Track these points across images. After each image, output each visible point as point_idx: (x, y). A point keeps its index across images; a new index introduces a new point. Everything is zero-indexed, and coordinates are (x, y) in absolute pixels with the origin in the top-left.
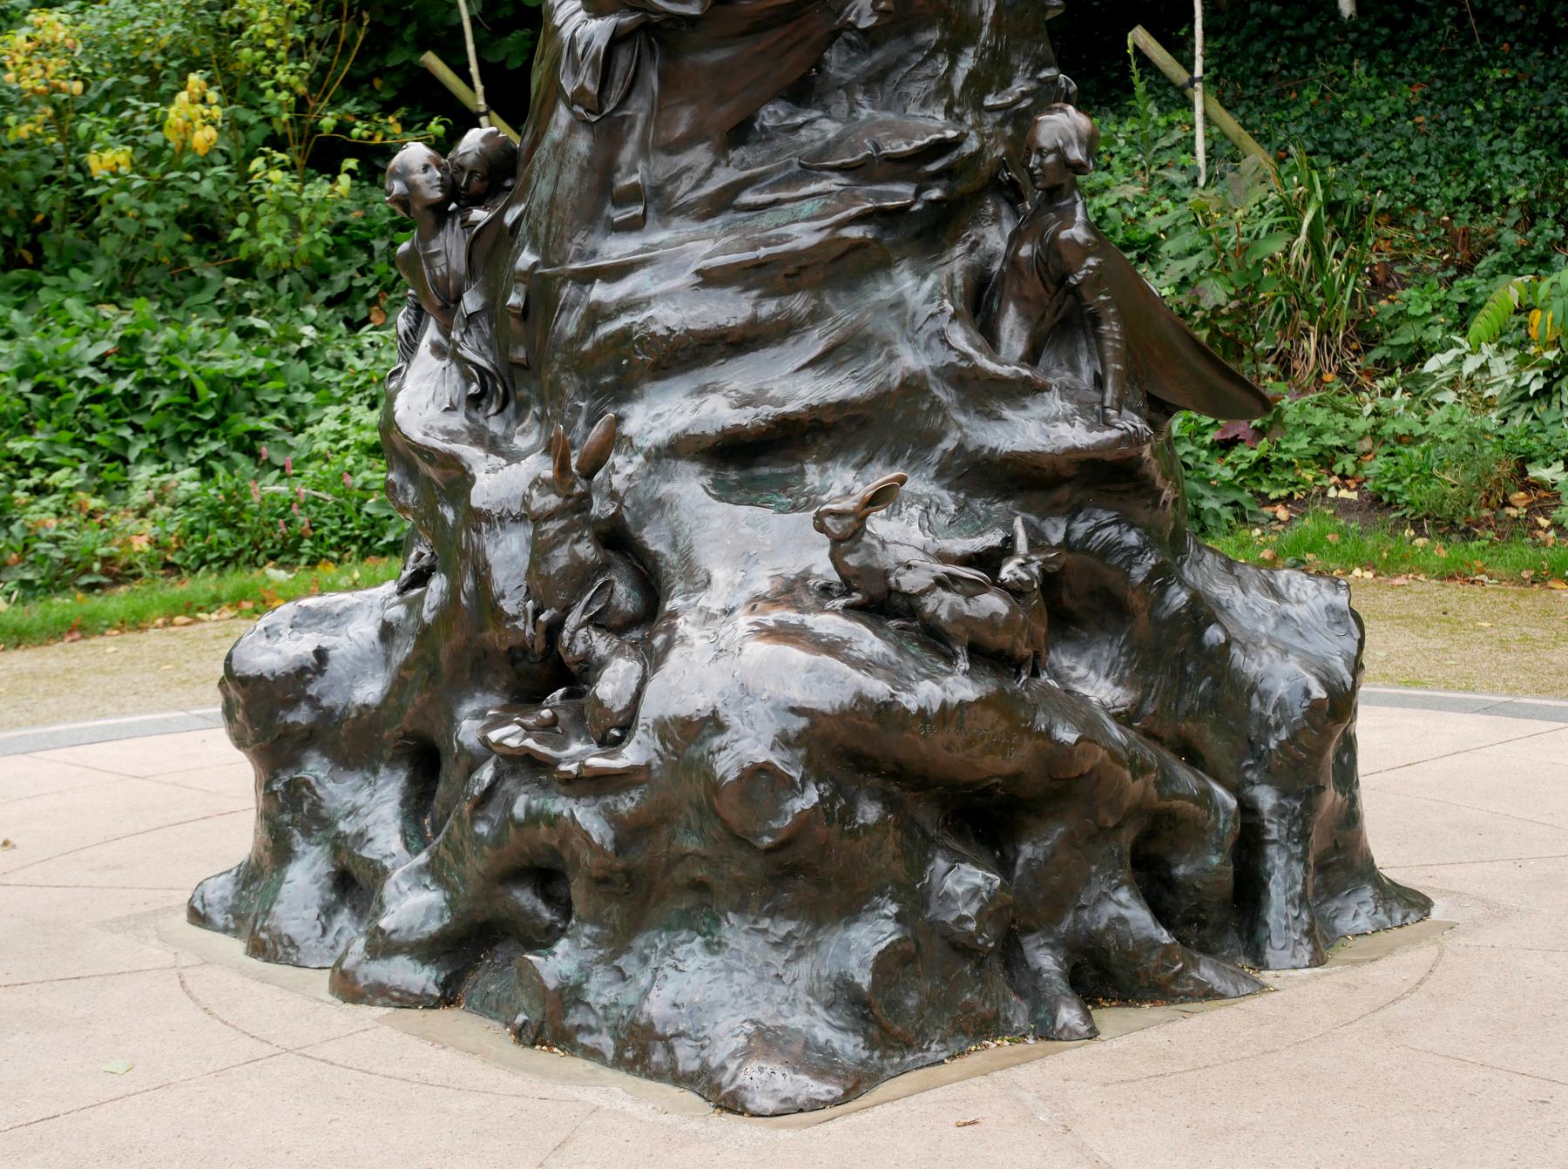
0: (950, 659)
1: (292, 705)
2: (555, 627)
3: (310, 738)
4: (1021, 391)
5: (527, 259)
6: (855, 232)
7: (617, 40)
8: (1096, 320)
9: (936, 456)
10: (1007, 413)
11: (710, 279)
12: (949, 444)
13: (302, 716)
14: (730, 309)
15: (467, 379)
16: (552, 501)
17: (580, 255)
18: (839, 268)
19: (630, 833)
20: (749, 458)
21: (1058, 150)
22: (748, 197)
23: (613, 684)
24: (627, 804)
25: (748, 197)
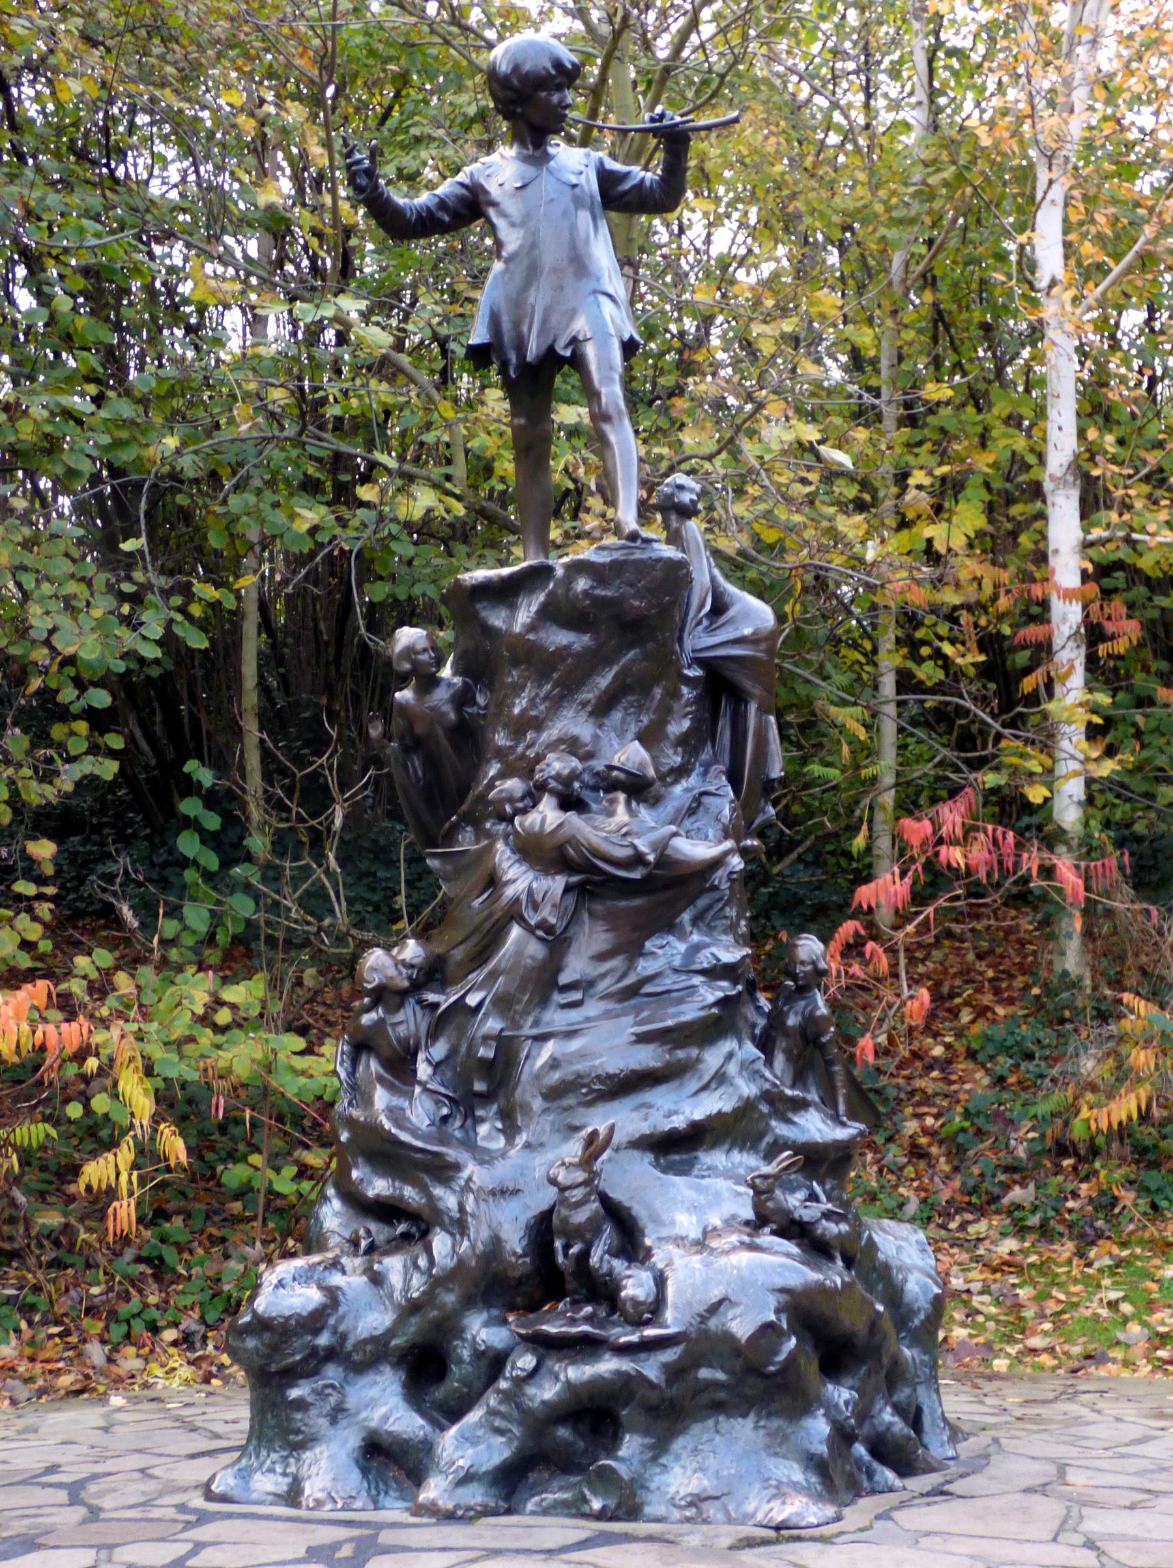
0: (831, 1259)
1: (317, 1332)
2: (585, 1254)
3: (331, 1354)
4: (800, 1105)
5: (493, 1025)
6: (715, 1010)
7: (568, 889)
8: (829, 1063)
9: (763, 1145)
10: (796, 1119)
11: (643, 1039)
12: (768, 1139)
13: (324, 1340)
14: (648, 1057)
15: (437, 1103)
16: (580, 1176)
17: (536, 1024)
18: (707, 1031)
19: (675, 1373)
20: (675, 1148)
21: (813, 963)
22: (648, 989)
23: (636, 1285)
24: (669, 1355)
25: (648, 989)
